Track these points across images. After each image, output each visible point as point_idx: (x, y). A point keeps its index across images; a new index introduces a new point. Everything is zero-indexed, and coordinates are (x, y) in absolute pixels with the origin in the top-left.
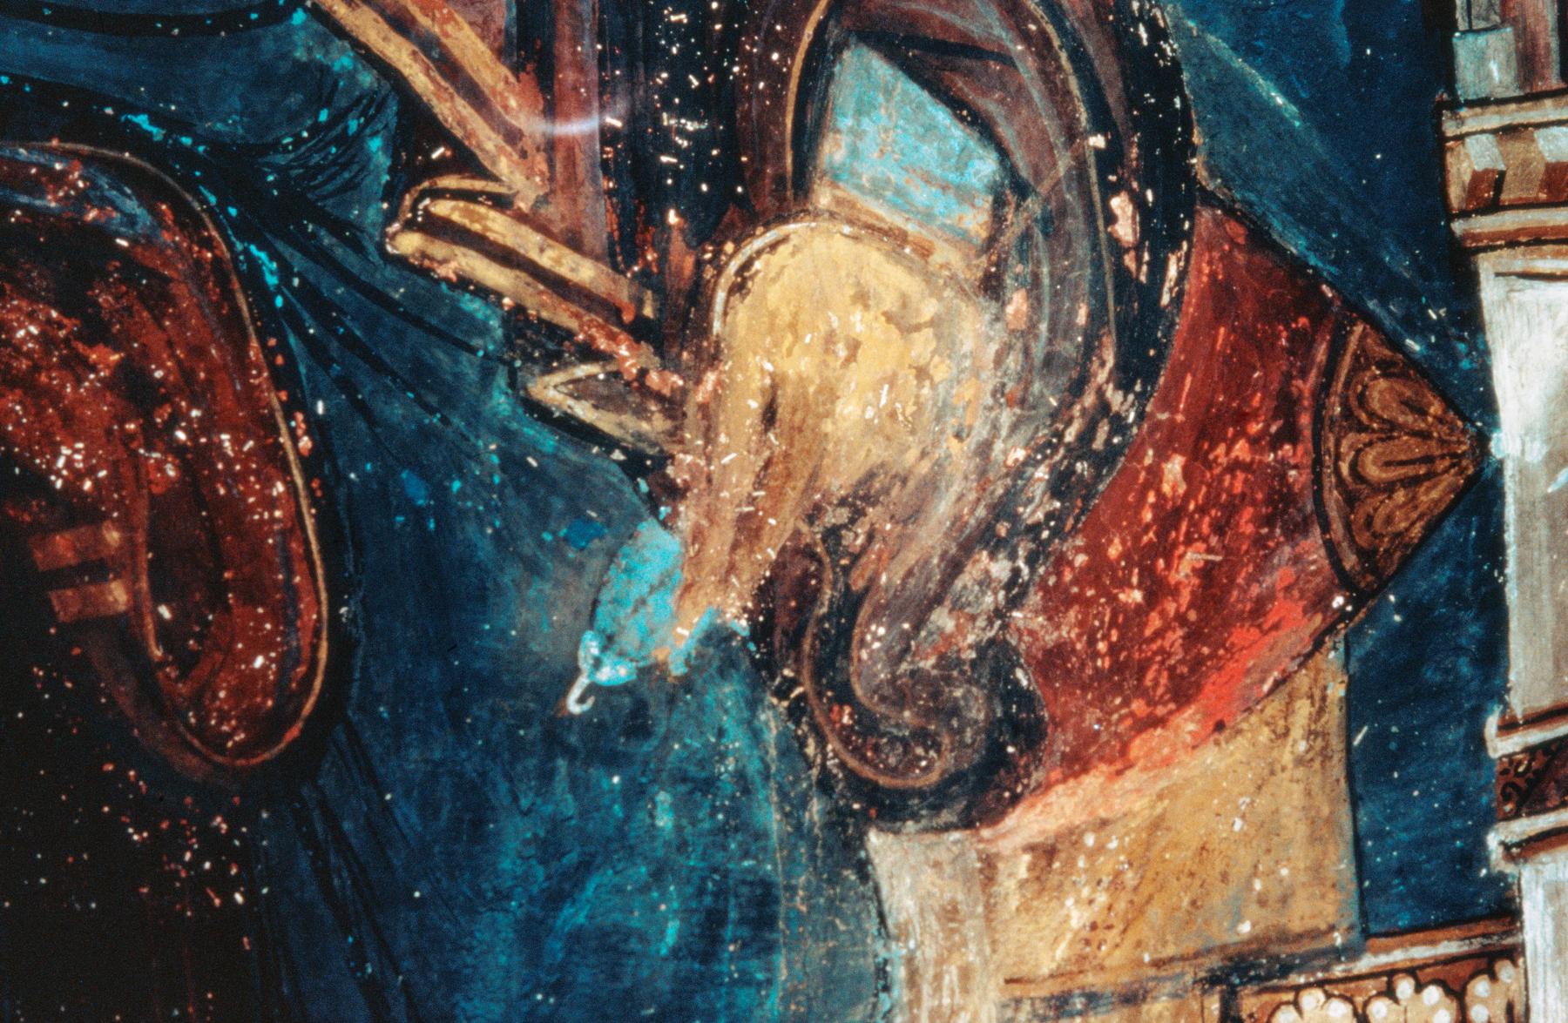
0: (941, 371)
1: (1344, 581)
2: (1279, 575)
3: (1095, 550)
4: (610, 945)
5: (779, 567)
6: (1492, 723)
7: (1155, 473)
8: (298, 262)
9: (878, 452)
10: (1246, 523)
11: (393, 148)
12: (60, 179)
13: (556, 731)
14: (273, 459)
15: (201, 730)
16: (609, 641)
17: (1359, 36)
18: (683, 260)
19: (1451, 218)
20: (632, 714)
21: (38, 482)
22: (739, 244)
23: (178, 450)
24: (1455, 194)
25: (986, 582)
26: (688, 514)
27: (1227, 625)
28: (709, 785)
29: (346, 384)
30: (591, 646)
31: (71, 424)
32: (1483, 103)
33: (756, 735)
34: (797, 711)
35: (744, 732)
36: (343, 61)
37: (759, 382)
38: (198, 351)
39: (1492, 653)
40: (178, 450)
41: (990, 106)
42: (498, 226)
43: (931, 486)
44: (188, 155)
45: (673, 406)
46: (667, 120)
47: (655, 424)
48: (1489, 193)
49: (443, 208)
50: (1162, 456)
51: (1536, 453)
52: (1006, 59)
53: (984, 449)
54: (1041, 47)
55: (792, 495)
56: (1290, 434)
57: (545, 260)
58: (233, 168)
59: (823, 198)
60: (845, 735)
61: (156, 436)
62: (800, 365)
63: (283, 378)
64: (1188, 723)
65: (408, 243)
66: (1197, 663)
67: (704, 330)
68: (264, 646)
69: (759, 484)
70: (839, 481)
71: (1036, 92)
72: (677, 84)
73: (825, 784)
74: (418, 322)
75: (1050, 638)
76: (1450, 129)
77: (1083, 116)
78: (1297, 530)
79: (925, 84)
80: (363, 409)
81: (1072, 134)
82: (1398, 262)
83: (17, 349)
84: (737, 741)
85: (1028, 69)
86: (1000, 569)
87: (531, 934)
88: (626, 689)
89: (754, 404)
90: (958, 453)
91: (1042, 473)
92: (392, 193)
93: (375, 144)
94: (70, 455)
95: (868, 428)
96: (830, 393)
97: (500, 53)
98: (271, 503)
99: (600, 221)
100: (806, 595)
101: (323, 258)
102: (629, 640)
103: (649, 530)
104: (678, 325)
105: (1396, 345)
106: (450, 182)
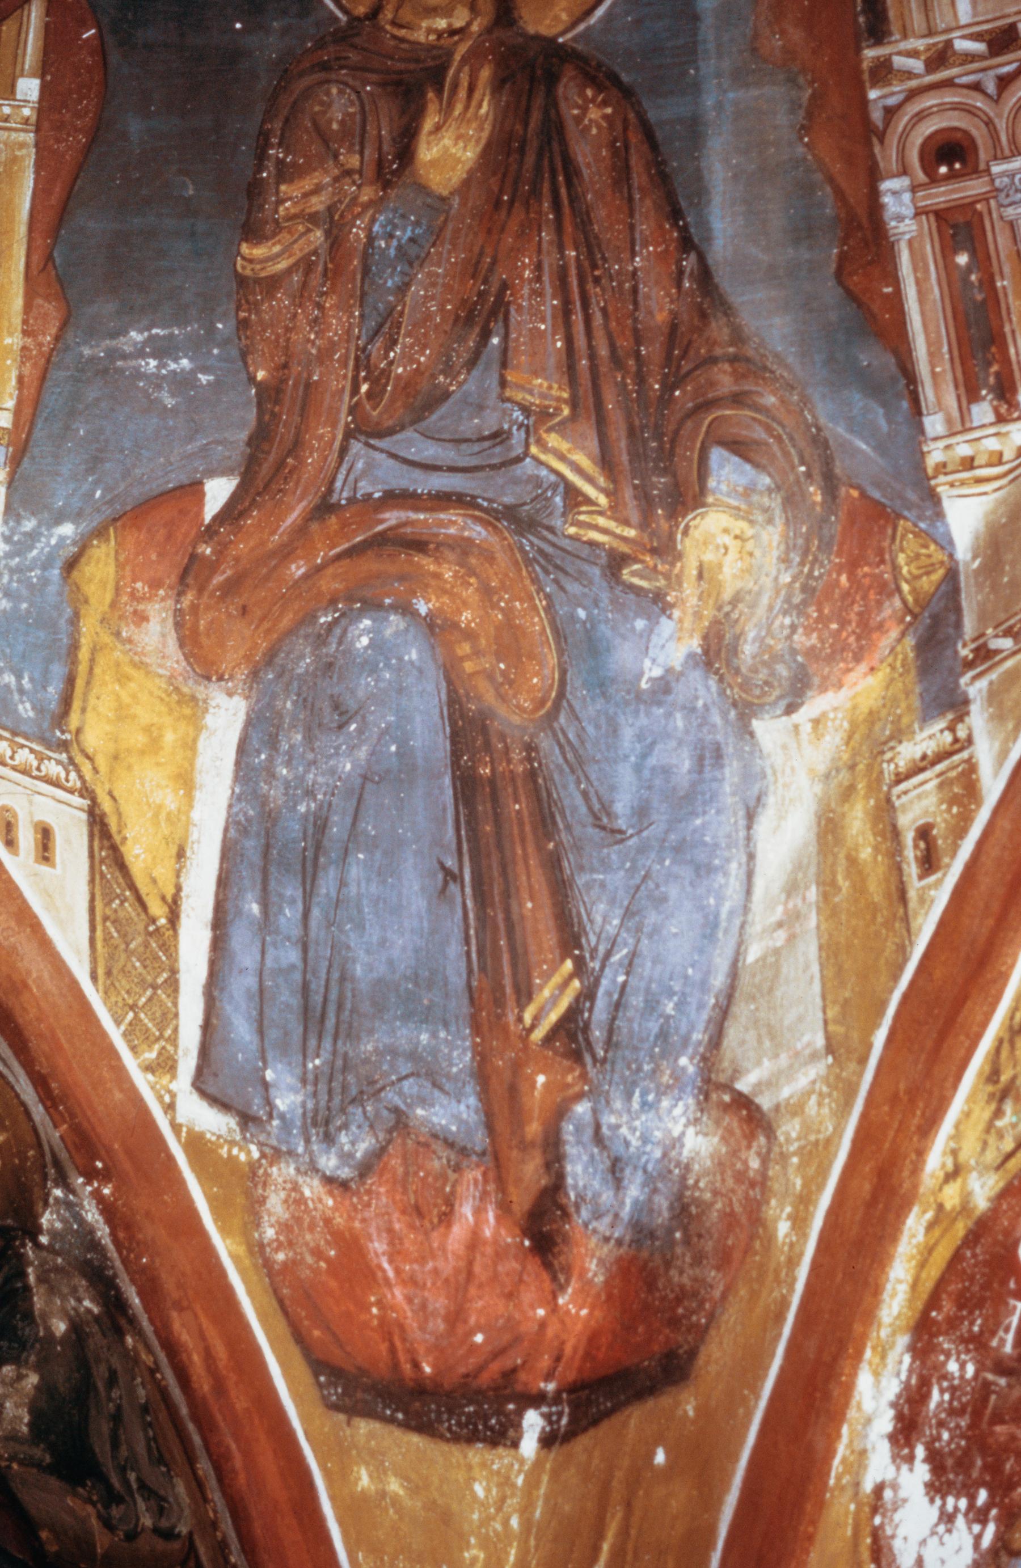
0: (758, 553)
1: (910, 612)
2: (887, 612)
3: (820, 610)
4: (666, 771)
5: (709, 628)
6: (960, 645)
7: (837, 581)
8: (536, 541)
9: (739, 584)
10: (872, 596)
11: (564, 500)
12: (454, 523)
13: (639, 696)
14: (535, 608)
15: (518, 706)
16: (654, 661)
17: (889, 421)
18: (664, 525)
19: (929, 479)
20: (664, 687)
21: (456, 625)
22: (684, 517)
23: (502, 610)
24: (930, 472)
25: (782, 626)
26: (676, 613)
27: (870, 632)
28: (693, 709)
29: (556, 581)
30: (647, 663)
31: (465, 604)
32: (935, 439)
33: (708, 688)
34: (721, 680)
35: (703, 689)
36: (544, 472)
37: (695, 564)
38: (506, 575)
39: (958, 625)
40: (502, 610)
41: (764, 461)
42: (601, 521)
43: (759, 593)
44: (496, 511)
45: (667, 576)
46: (654, 479)
47: (662, 583)
48: (942, 468)
49: (582, 518)
50: (839, 574)
51: (969, 556)
52: (767, 444)
53: (776, 579)
54: (779, 439)
55: (711, 602)
56: (882, 561)
57: (618, 531)
58: (510, 513)
59: (710, 499)
60: (741, 686)
61: (495, 606)
62: (709, 557)
63: (536, 580)
64: (863, 667)
65: (572, 530)
66: (861, 648)
67: (675, 547)
68: (537, 674)
69: (700, 599)
70: (727, 595)
71: (779, 454)
72: (656, 467)
73: (735, 704)
74: (578, 557)
75: (808, 644)
76: (925, 449)
77: (796, 461)
78: (890, 595)
79: (740, 456)
80: (562, 589)
81: (793, 468)
82: (912, 496)
83: (446, 581)
84: (702, 691)
85: (775, 448)
86: (787, 621)
87: (638, 769)
88: (662, 678)
89: (695, 572)
90: (767, 582)
91: (797, 585)
92: (564, 514)
93: (558, 499)
94: (466, 616)
95: (735, 576)
96: (720, 566)
97: (595, 463)
98: (534, 624)
99: (635, 516)
100: (720, 637)
101: (544, 539)
102: (661, 660)
103: (663, 620)
104: (665, 549)
105: (915, 525)
106: (584, 508)
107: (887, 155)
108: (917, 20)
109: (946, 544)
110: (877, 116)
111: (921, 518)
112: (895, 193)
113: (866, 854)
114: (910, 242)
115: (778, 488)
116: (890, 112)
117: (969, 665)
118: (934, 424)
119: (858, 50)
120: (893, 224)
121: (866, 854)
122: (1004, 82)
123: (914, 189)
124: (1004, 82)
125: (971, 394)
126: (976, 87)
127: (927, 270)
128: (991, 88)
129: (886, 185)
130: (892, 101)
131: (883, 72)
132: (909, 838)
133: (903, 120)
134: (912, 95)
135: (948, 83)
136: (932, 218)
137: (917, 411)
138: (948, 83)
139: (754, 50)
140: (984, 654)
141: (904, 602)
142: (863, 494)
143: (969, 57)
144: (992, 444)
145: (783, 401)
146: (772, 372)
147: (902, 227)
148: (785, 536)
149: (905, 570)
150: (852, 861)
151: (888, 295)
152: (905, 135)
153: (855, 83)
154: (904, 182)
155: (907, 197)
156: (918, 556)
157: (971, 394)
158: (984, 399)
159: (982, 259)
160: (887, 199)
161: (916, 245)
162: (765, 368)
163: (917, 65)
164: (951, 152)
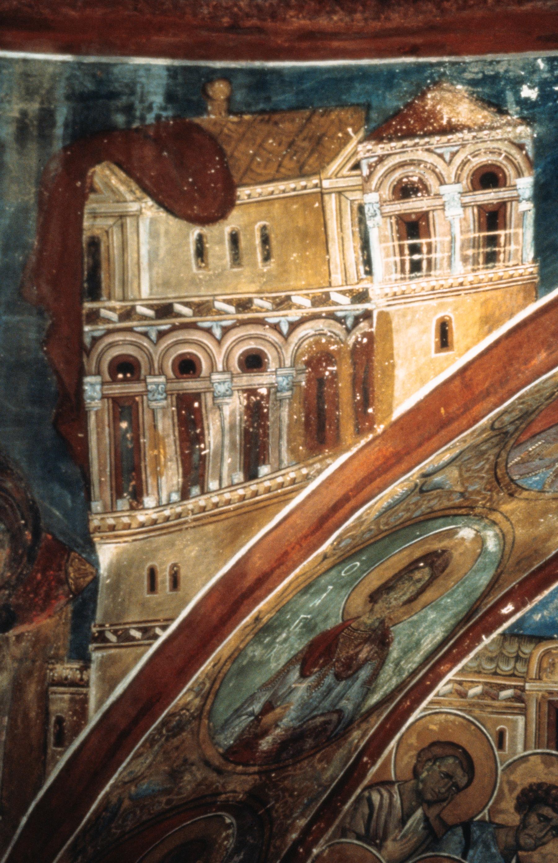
2: (61, 591)
6: (93, 624)
17: (73, 502)
24: (91, 530)
25: (4, 595)
32: (97, 514)
48: (98, 529)
51: (105, 574)
52: (5, 509)
54: (11, 506)
56: (60, 570)
64: (45, 615)
76: (90, 518)
77: (19, 516)
81: (17, 521)
86: (7, 592)
107: (91, 364)
108: (118, 291)
109: (95, 564)
110: (87, 340)
111: (83, 552)
112: (92, 385)
113: (33, 714)
114: (97, 413)
115: (8, 530)
116: (95, 340)
117: (95, 640)
118: (97, 506)
119: (81, 303)
120: (88, 401)
121: (33, 714)
122: (161, 334)
123: (103, 383)
124: (161, 334)
125: (118, 493)
126: (146, 334)
127: (103, 428)
128: (153, 336)
129: (88, 379)
130: (97, 334)
131: (94, 317)
132: (53, 719)
133: (101, 346)
134: (109, 332)
135: (130, 330)
136: (110, 401)
137: (88, 499)
138: (130, 330)
139: (20, 294)
140: (101, 638)
141: (70, 589)
142: (54, 538)
143: (144, 317)
144: (126, 520)
145: (16, 486)
146: (12, 470)
147: (93, 404)
148: (9, 556)
149: (72, 575)
150: (26, 715)
151: (81, 438)
152: (103, 352)
153: (77, 320)
154: (98, 379)
155: (98, 388)
156: (79, 569)
157: (118, 493)
158: (124, 498)
159: (135, 426)
160: (86, 388)
161: (100, 414)
162: (8, 468)
163: (114, 316)
164: (126, 367)
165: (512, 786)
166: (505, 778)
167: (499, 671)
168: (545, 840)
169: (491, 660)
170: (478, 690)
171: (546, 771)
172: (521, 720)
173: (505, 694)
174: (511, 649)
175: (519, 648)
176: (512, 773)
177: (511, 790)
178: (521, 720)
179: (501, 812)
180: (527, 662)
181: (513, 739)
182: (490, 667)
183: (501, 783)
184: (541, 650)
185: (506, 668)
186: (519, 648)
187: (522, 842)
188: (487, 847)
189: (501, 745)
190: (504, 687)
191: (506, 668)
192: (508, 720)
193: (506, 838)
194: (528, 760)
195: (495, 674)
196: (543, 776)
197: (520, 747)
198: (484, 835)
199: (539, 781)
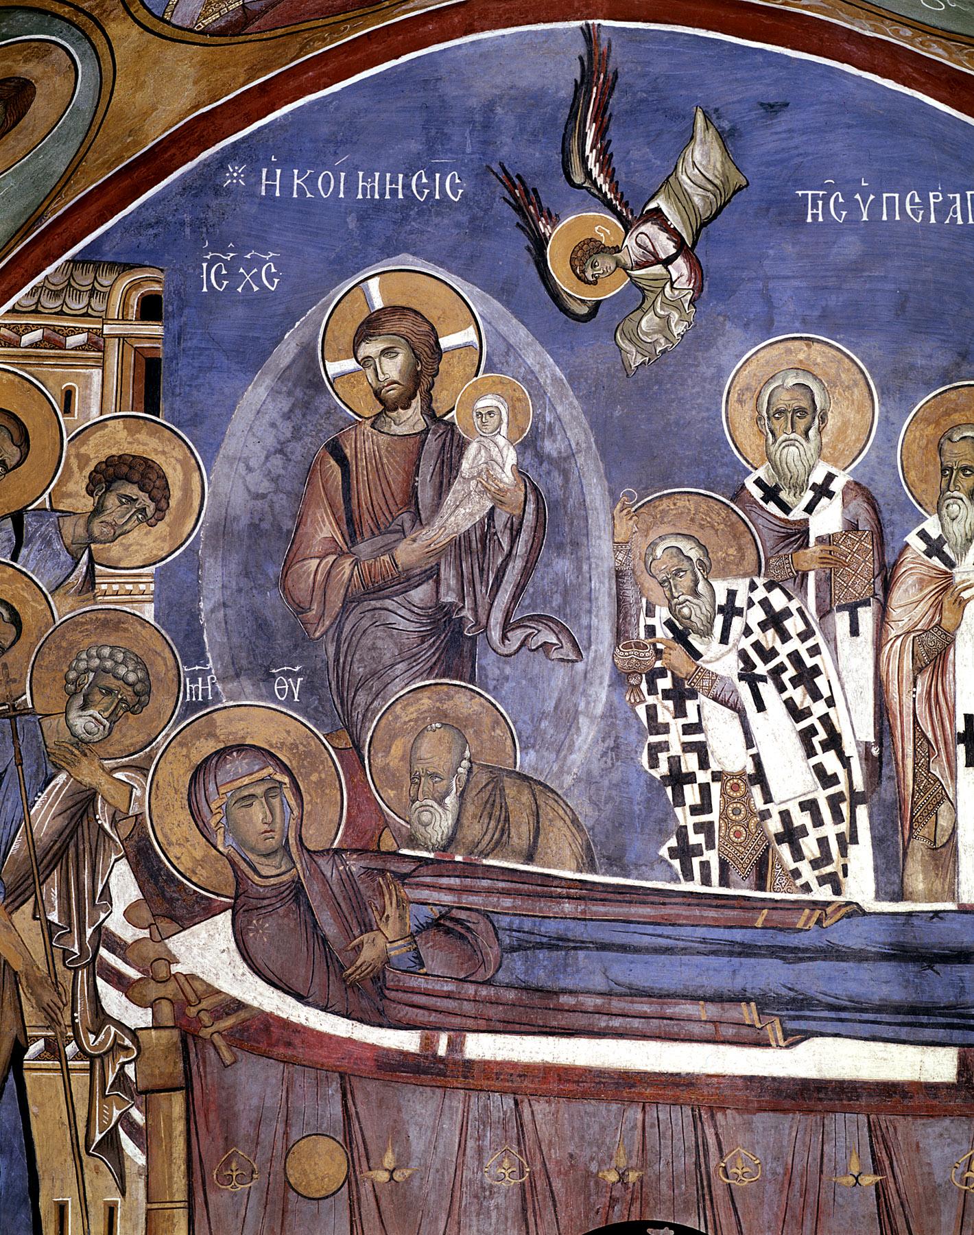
165: (83, 460)
166: (73, 451)
167: (65, 309)
168: (127, 528)
169: (56, 294)
170: (36, 335)
171: (130, 439)
172: (96, 374)
173: (72, 341)
174: (84, 279)
175: (95, 278)
176: (83, 443)
177: (81, 469)
178: (96, 374)
179: (70, 495)
180: (106, 296)
181: (85, 400)
182: (51, 304)
183: (68, 458)
184: (126, 281)
185: (77, 305)
186: (95, 278)
187: (96, 531)
188: (49, 543)
189: (67, 409)
190: (75, 331)
191: (77, 305)
192: (78, 375)
193: (73, 529)
194: (107, 426)
195: (61, 313)
196: (126, 445)
197: (95, 410)
198: (43, 529)
199: (121, 453)
